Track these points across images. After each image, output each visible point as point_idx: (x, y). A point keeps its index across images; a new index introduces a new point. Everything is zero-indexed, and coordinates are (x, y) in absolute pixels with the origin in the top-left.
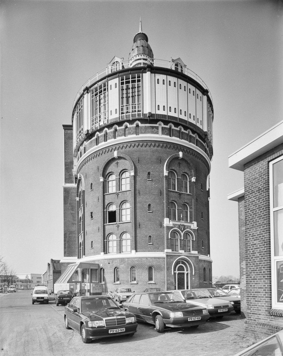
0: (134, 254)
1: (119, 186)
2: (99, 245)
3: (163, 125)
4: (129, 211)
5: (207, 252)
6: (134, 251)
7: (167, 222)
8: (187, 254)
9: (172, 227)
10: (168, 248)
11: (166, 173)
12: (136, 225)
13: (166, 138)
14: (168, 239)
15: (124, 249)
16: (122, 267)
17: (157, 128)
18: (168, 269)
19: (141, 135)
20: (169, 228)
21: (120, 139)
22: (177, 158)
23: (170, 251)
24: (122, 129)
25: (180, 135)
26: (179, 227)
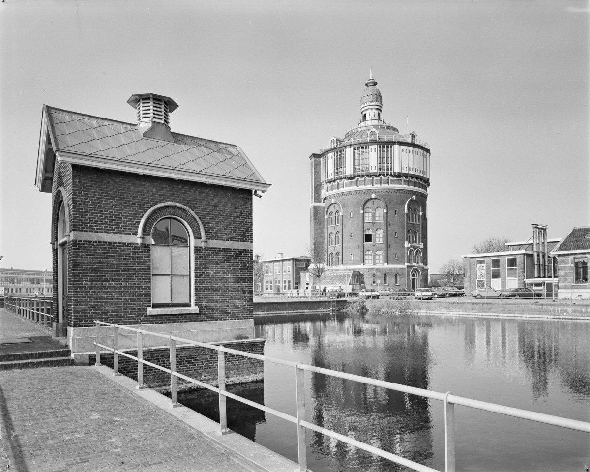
0: (386, 266)
1: (374, 217)
2: (360, 258)
3: (405, 179)
4: (381, 236)
5: (426, 264)
6: (386, 264)
7: (407, 244)
8: (417, 265)
9: (410, 248)
10: (407, 262)
11: (406, 211)
12: (388, 246)
13: (406, 187)
14: (407, 256)
15: (366, 261)
16: (378, 274)
17: (401, 180)
18: (408, 276)
19: (390, 185)
20: (408, 248)
21: (377, 186)
22: (412, 200)
23: (408, 264)
24: (370, 180)
25: (415, 184)
26: (413, 247)
